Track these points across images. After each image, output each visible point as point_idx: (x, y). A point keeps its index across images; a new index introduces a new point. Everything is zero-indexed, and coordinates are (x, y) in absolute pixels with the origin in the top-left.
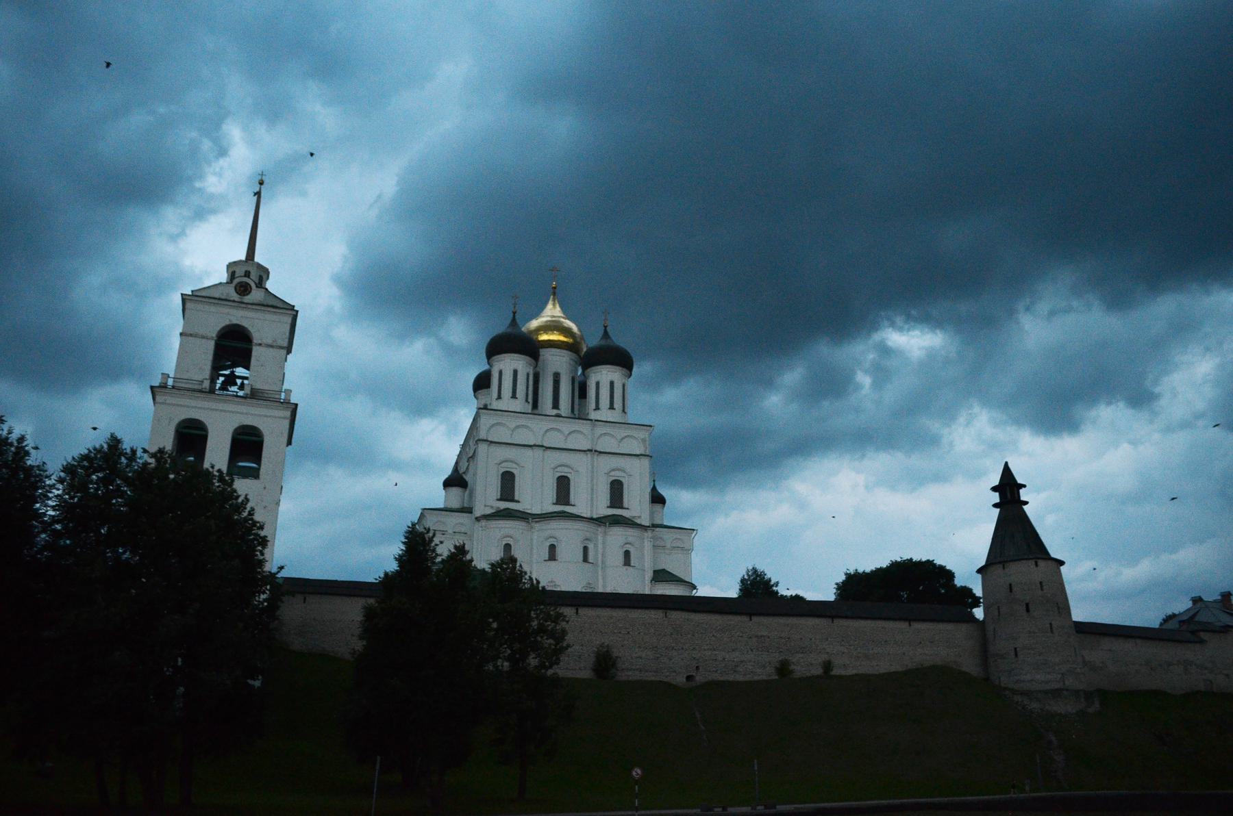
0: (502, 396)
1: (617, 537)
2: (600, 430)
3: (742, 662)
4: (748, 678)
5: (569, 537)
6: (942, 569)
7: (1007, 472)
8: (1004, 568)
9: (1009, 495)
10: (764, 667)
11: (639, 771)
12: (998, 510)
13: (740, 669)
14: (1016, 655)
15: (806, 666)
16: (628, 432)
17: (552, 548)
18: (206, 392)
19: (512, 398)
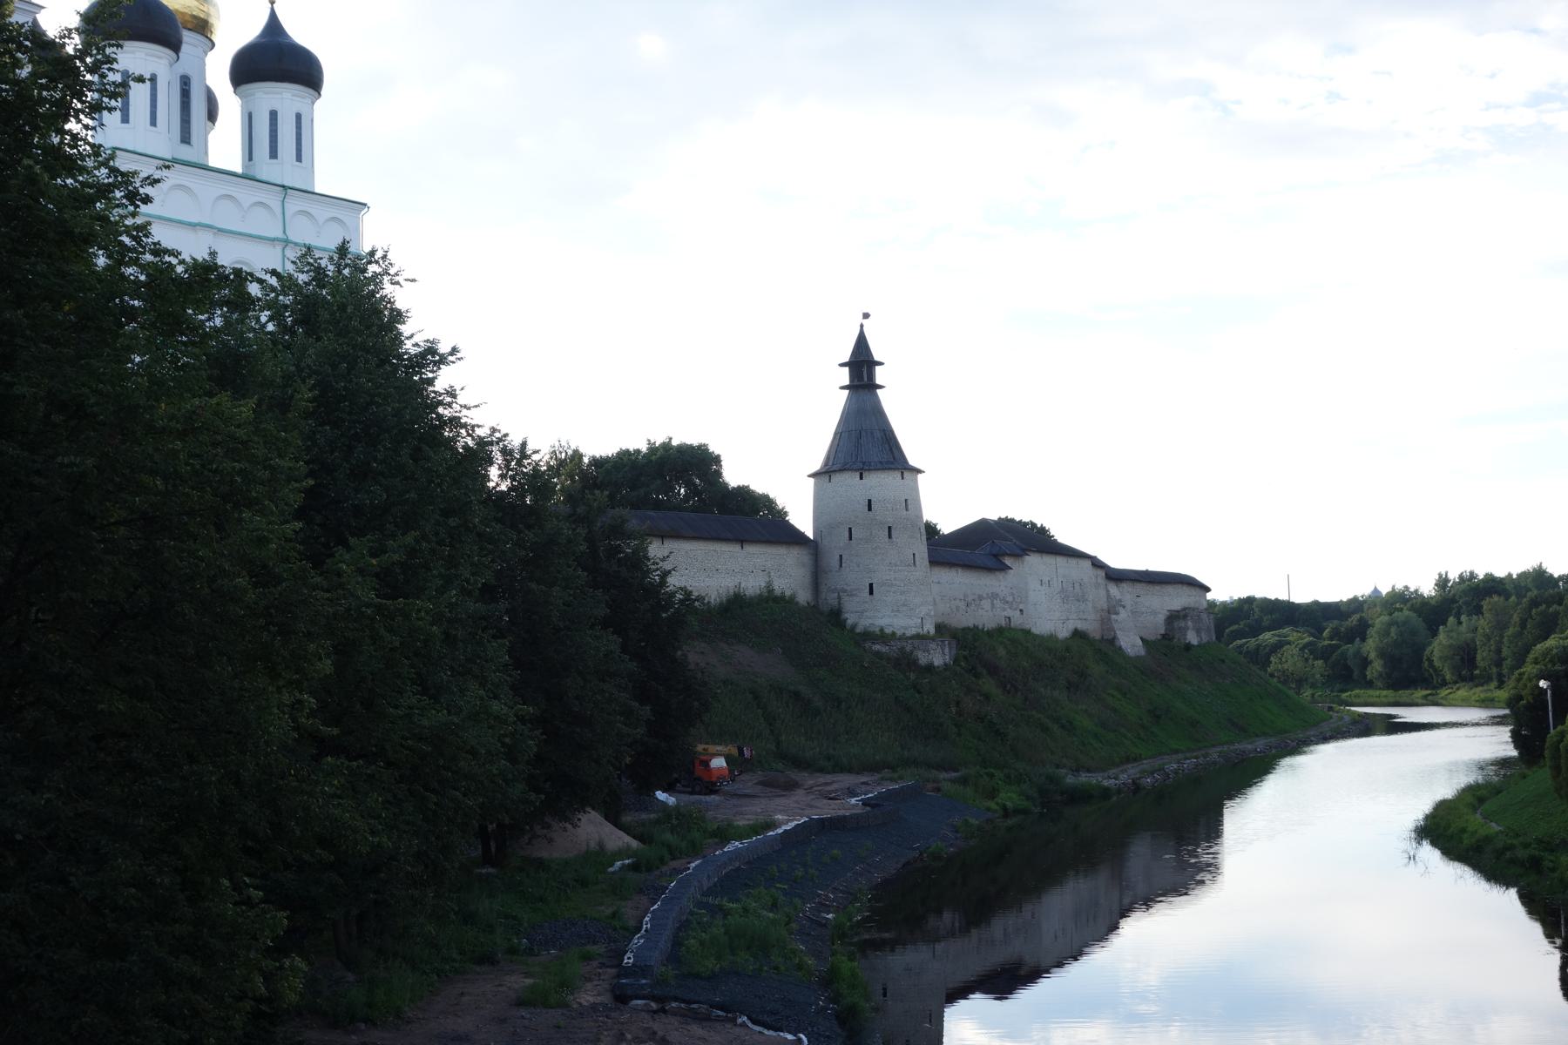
2: (295, 204)
7: (862, 345)
8: (861, 478)
9: (866, 379)
12: (847, 392)
14: (871, 592)
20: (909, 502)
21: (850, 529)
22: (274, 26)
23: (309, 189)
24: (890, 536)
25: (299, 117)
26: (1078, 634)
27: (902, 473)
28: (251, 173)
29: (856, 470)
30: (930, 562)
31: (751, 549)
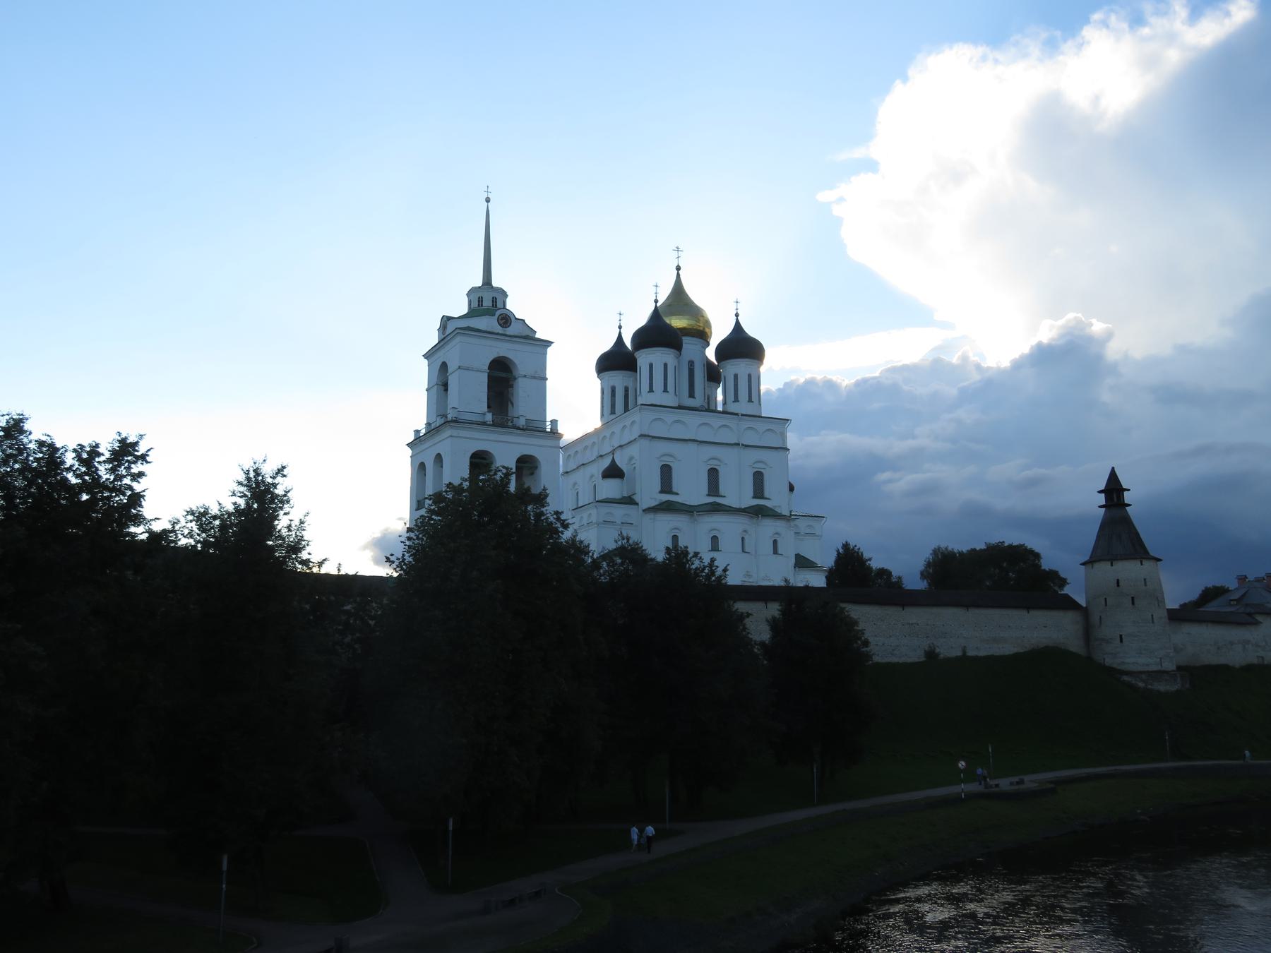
1: (768, 528)
5: (729, 528)
6: (1031, 552)
7: (1113, 477)
8: (1112, 565)
9: (1115, 500)
11: (963, 763)
13: (895, 652)
14: (1121, 641)
15: (948, 649)
17: (715, 539)
18: (489, 425)
19: (664, 391)
21: (1106, 599)
22: (738, 327)
23: (757, 414)
24: (1133, 603)
25: (750, 376)
28: (725, 410)
29: (1108, 560)
31: (1034, 613)
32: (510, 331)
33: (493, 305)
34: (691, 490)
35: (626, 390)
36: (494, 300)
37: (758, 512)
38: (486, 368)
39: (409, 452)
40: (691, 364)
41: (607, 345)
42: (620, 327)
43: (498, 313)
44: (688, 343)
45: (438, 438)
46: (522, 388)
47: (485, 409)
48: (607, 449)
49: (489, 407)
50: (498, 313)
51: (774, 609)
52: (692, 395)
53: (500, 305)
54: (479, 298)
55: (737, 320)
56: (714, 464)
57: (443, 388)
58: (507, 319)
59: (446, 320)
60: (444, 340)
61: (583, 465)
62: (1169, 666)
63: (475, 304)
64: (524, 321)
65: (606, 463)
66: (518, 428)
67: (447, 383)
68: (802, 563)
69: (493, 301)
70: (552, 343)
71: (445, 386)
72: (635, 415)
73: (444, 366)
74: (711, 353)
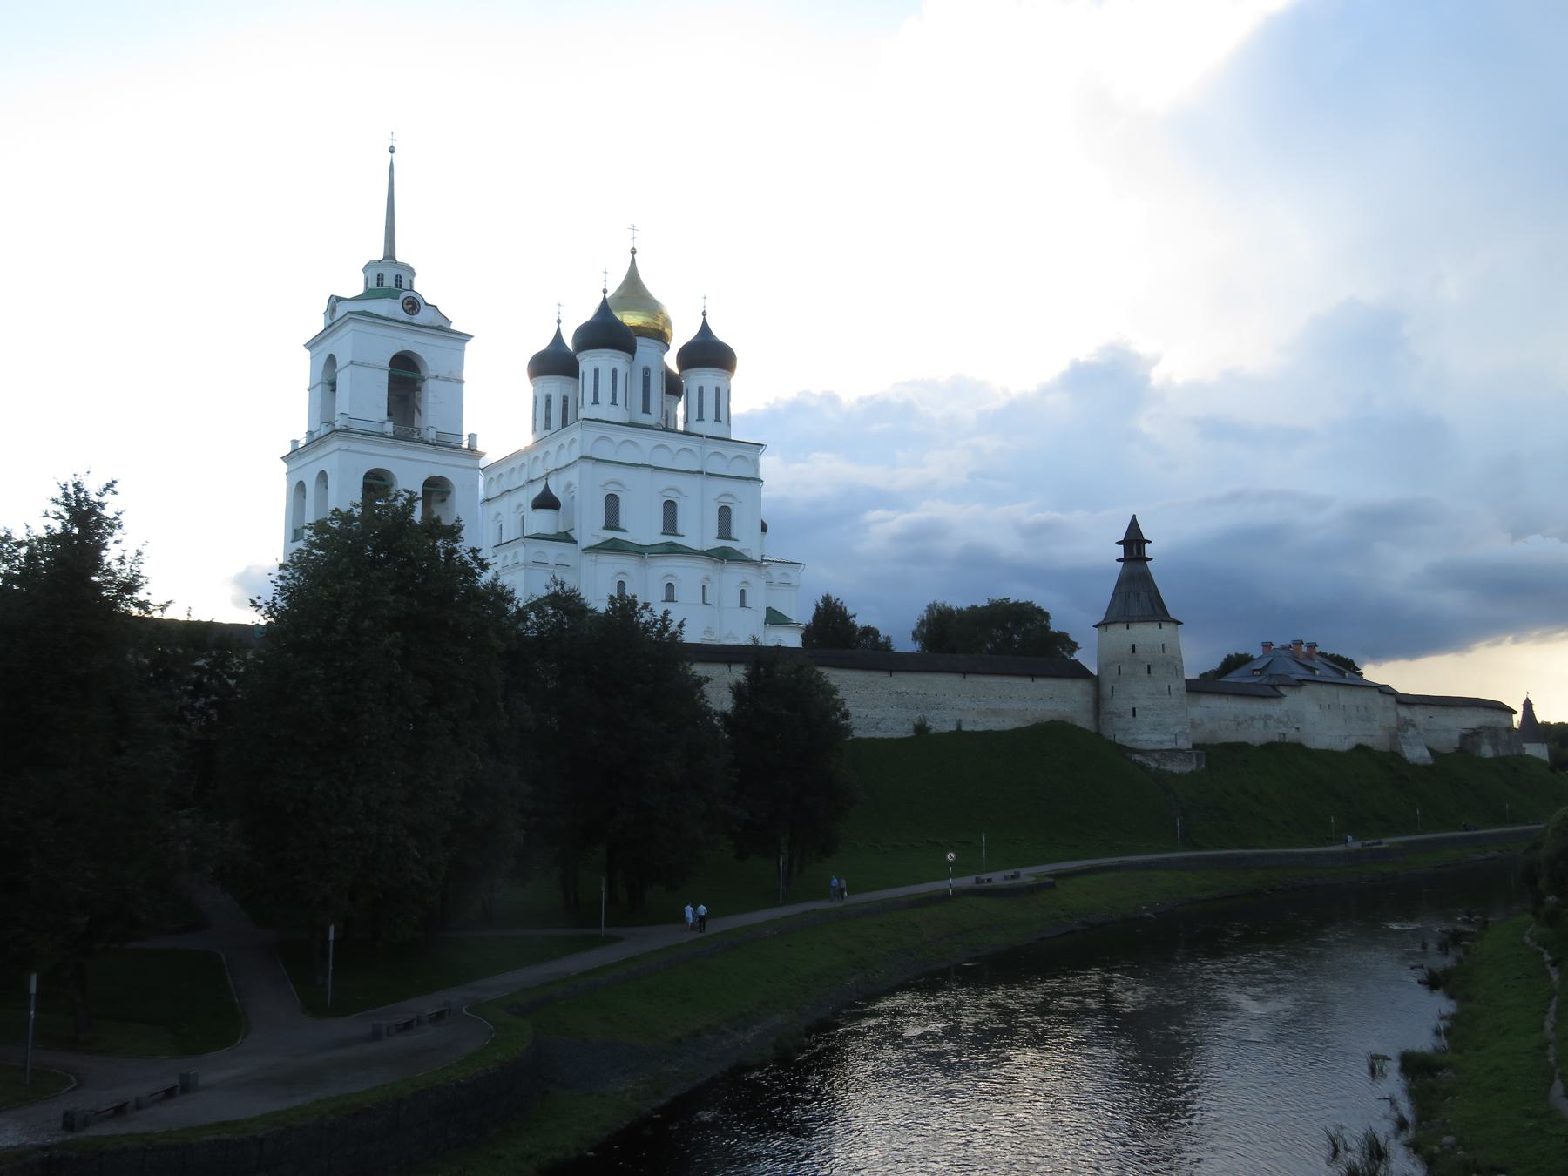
0: (600, 400)
1: (734, 575)
3: (883, 719)
4: (886, 735)
5: (688, 574)
6: (1040, 611)
7: (1134, 525)
8: (1128, 628)
10: (903, 723)
11: (953, 855)
14: (1134, 715)
15: (942, 723)
16: (740, 452)
17: (670, 587)
18: (389, 437)
20: (1166, 646)
21: (1119, 667)
22: (705, 329)
23: (726, 437)
24: (1149, 672)
25: (718, 390)
26: (1360, 748)
27: (1160, 624)
29: (1124, 622)
30: (1187, 691)
31: (1041, 682)
32: (417, 319)
33: (397, 285)
34: (642, 526)
35: (565, 400)
36: (398, 279)
37: (724, 556)
38: (386, 364)
39: (284, 467)
40: (647, 371)
41: (542, 343)
42: (559, 321)
43: (403, 295)
44: (642, 345)
45: (322, 452)
46: (432, 394)
47: (383, 415)
48: (539, 472)
49: (389, 414)
50: (403, 295)
51: (738, 673)
52: (646, 410)
53: (405, 285)
54: (379, 275)
55: (704, 319)
56: (671, 495)
57: (329, 388)
58: (414, 305)
59: (335, 301)
60: (331, 328)
61: (509, 491)
62: (1184, 744)
63: (373, 283)
64: (436, 307)
65: (538, 490)
66: (427, 443)
67: (335, 382)
68: (774, 618)
69: (397, 280)
70: (472, 337)
71: (333, 386)
72: (575, 433)
73: (331, 360)
74: (671, 360)
